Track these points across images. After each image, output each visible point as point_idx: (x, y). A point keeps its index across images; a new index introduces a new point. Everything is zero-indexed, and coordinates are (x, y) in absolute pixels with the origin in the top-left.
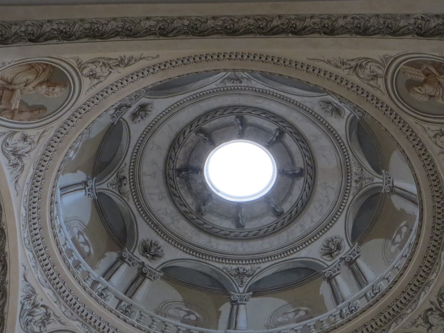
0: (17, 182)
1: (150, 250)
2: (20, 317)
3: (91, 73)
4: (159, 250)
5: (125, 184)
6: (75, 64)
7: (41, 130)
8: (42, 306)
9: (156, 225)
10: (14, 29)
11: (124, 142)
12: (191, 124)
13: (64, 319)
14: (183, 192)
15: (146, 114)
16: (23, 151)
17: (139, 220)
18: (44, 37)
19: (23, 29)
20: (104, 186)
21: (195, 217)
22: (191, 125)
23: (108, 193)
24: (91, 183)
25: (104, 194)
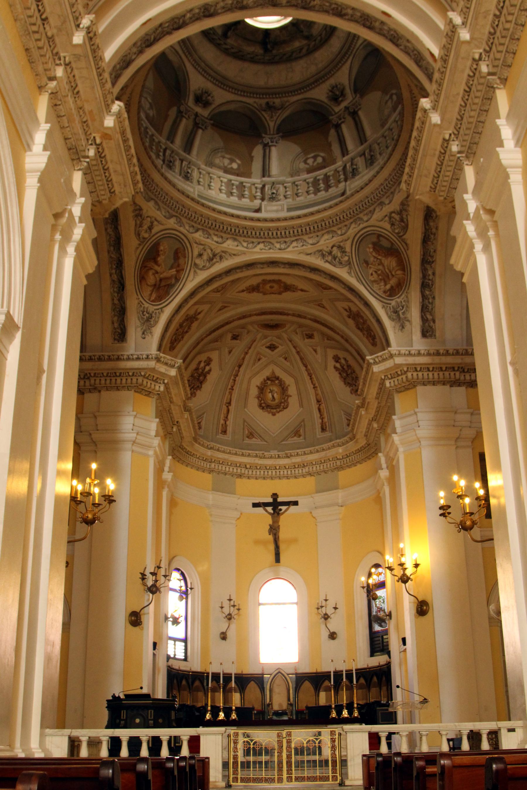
0: (234, 255)
1: (336, 95)
2: (334, 266)
3: (148, 230)
4: (339, 86)
5: (274, 103)
6: (141, 247)
7: (195, 245)
8: (332, 248)
9: (316, 81)
10: (116, 302)
11: (232, 107)
12: (218, 46)
13: (345, 237)
14: (288, 49)
15: (206, 92)
16: (210, 254)
17: (308, 95)
18: (120, 279)
19: (116, 295)
20: (272, 124)
21: (313, 43)
22: (219, 44)
23: (278, 122)
24: (267, 139)
25: (280, 125)
